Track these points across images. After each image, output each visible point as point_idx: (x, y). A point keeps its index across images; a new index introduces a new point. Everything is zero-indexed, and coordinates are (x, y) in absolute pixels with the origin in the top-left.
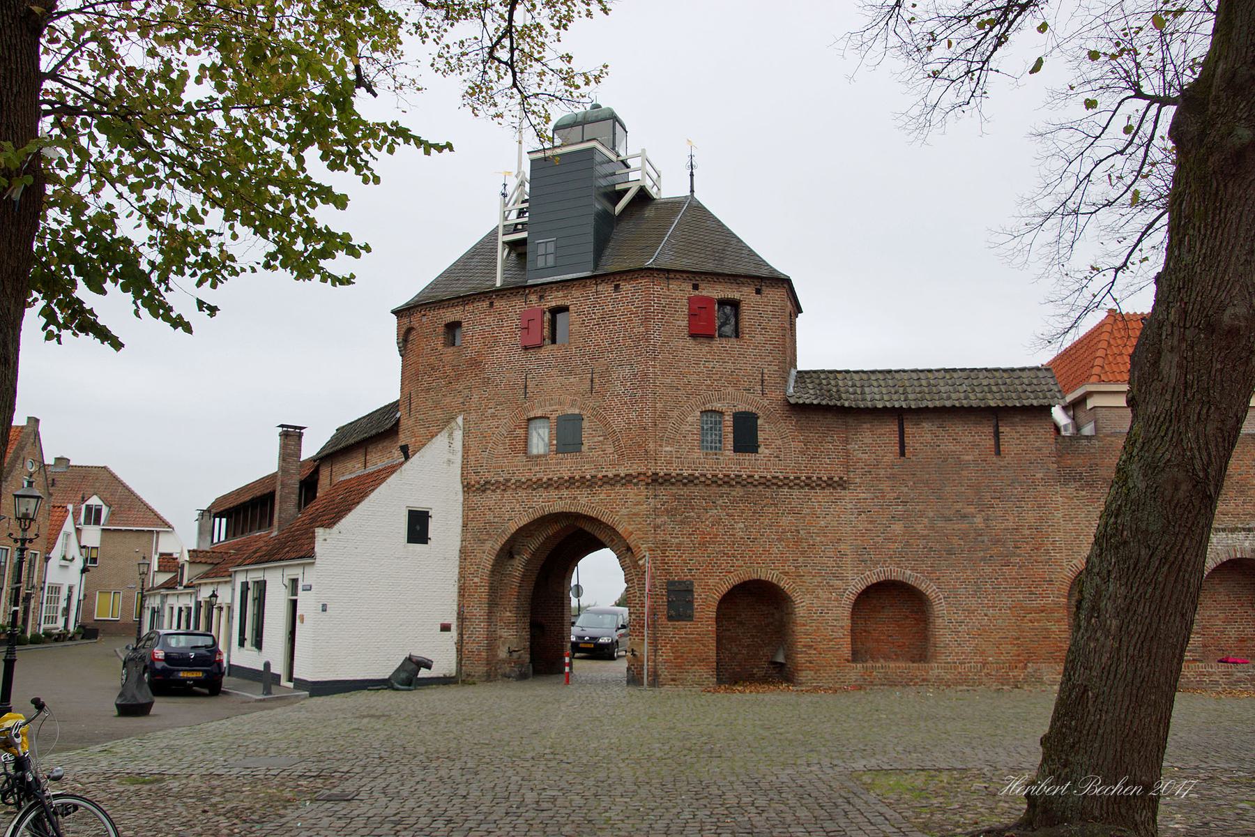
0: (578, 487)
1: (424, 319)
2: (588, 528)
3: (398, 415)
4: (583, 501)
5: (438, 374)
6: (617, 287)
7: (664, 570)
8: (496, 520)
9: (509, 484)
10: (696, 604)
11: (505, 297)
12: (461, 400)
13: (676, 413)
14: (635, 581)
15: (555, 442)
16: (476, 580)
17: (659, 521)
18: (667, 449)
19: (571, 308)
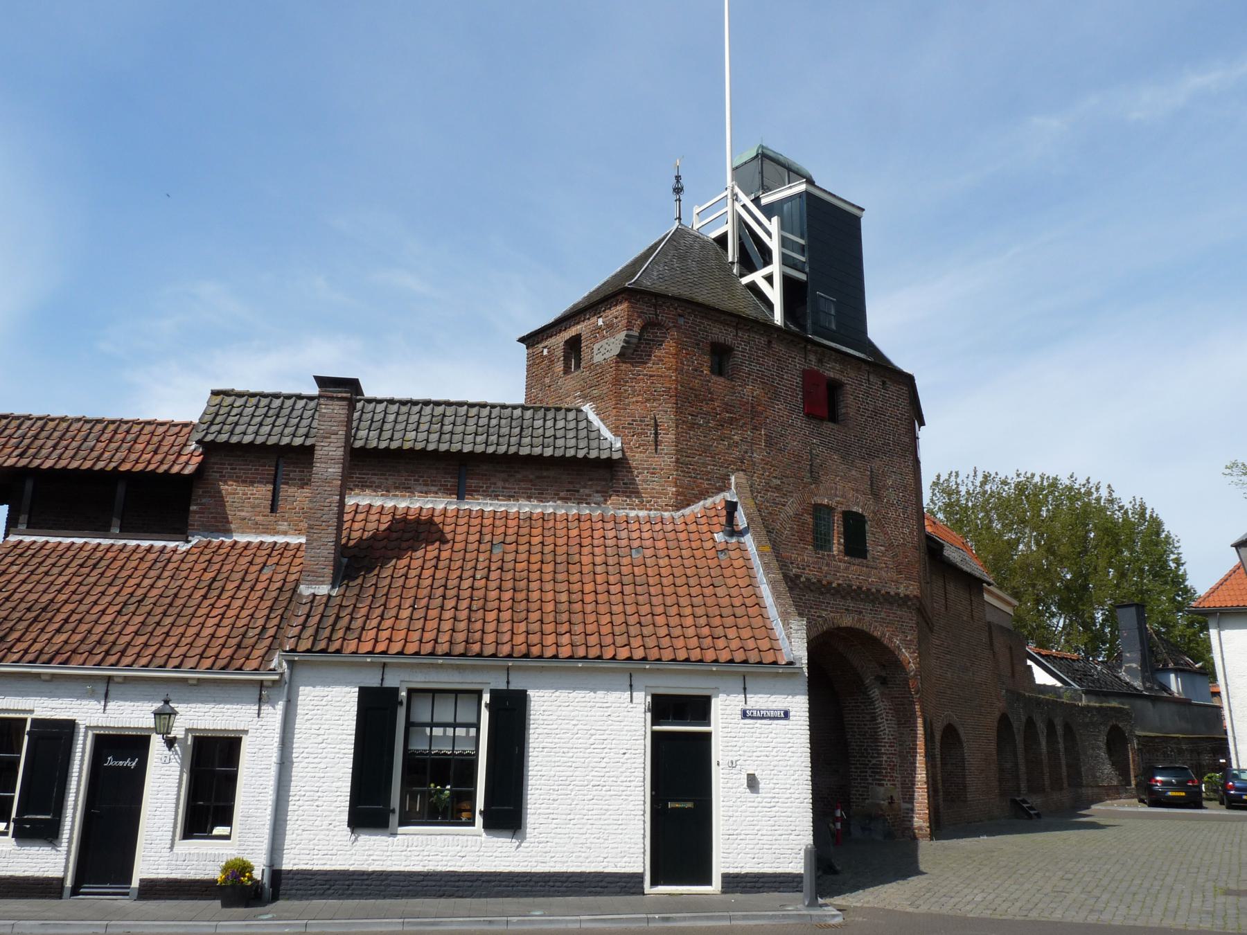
0: (862, 600)
1: (681, 321)
4: (868, 618)
6: (884, 383)
15: (842, 541)
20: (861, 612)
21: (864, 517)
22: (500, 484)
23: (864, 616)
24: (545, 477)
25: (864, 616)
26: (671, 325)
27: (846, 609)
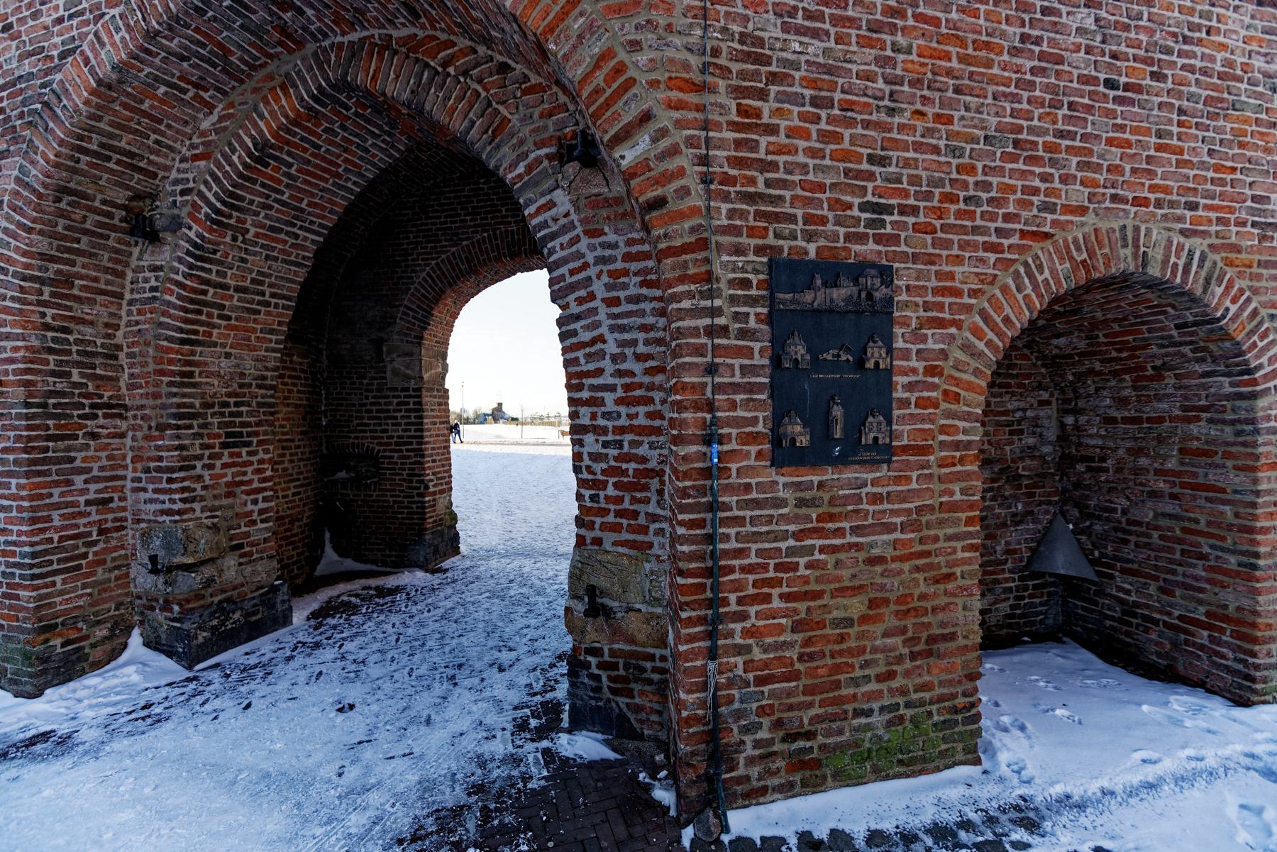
8: (27, 67)
10: (900, 380)
14: (598, 287)
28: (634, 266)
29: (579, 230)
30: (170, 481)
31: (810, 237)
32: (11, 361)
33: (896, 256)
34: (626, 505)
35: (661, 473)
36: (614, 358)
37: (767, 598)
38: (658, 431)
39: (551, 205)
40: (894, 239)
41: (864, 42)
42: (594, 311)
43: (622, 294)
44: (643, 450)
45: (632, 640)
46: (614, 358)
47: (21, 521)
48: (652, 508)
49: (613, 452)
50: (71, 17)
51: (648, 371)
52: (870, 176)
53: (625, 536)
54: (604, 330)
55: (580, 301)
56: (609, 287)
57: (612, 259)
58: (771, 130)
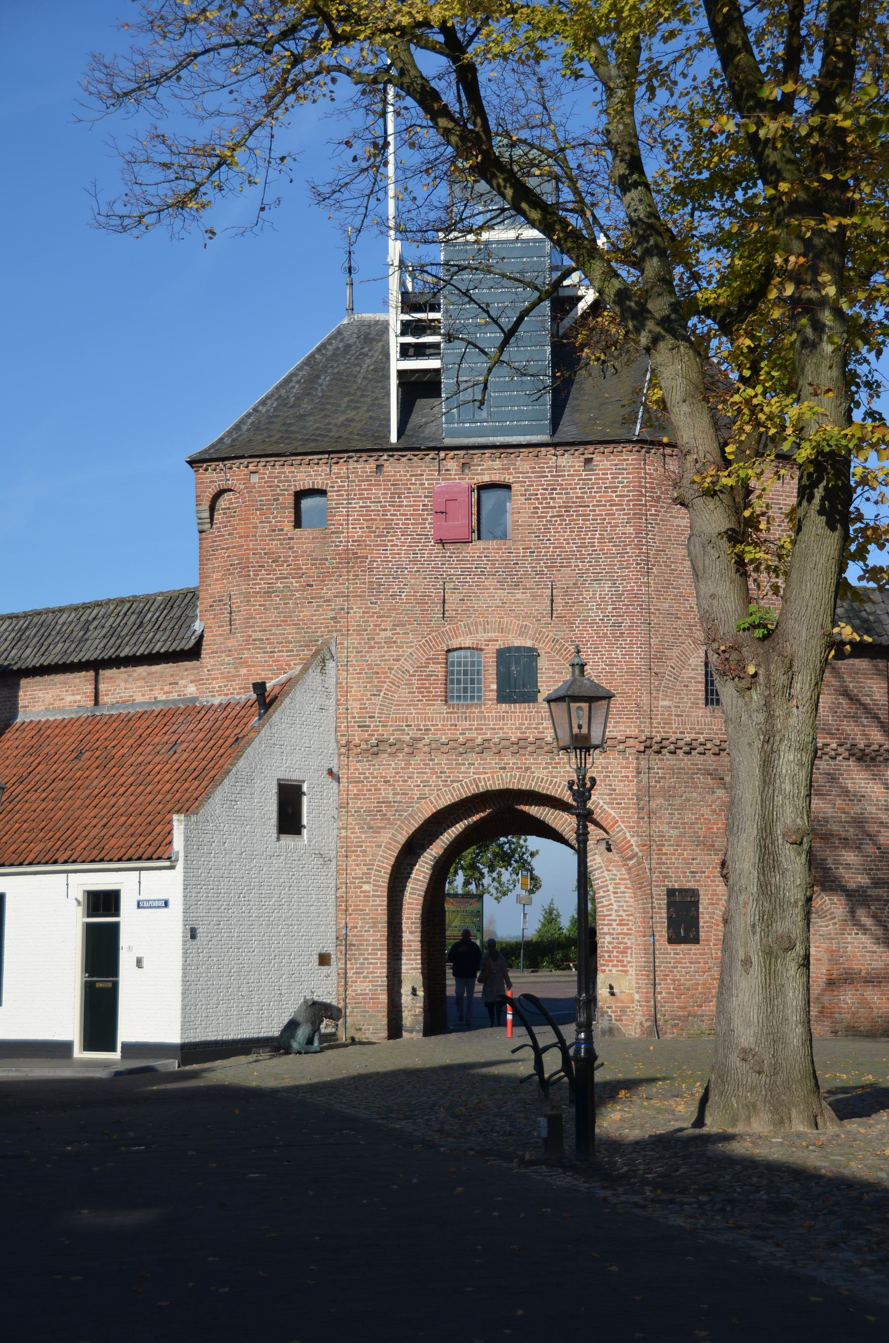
0: (532, 753)
1: (255, 478)
2: (534, 810)
3: (198, 626)
5: (285, 570)
6: (588, 461)
7: (660, 873)
8: (398, 798)
9: (420, 745)
11: (404, 459)
12: (331, 614)
13: (676, 652)
14: (611, 888)
16: (366, 887)
17: (653, 805)
18: (666, 703)
19: (515, 487)
20: (527, 769)
21: (536, 650)
22: (123, 685)
23: (533, 773)
24: (153, 673)
25: (533, 773)
26: (242, 487)
27: (500, 768)
28: (623, 882)
29: (604, 869)
30: (416, 955)
31: (676, 882)
32: (381, 905)
33: (699, 886)
34: (620, 958)
35: (631, 948)
36: (616, 911)
37: (666, 980)
38: (630, 934)
39: (595, 860)
40: (699, 881)
41: (690, 828)
42: (609, 895)
43: (619, 891)
44: (626, 940)
45: (622, 1002)
46: (616, 911)
47: (383, 968)
48: (629, 959)
49: (616, 941)
50: (424, 786)
51: (628, 915)
52: (692, 864)
53: (620, 968)
54: (612, 901)
55: (604, 892)
56: (614, 888)
57: (615, 879)
58: (666, 854)
